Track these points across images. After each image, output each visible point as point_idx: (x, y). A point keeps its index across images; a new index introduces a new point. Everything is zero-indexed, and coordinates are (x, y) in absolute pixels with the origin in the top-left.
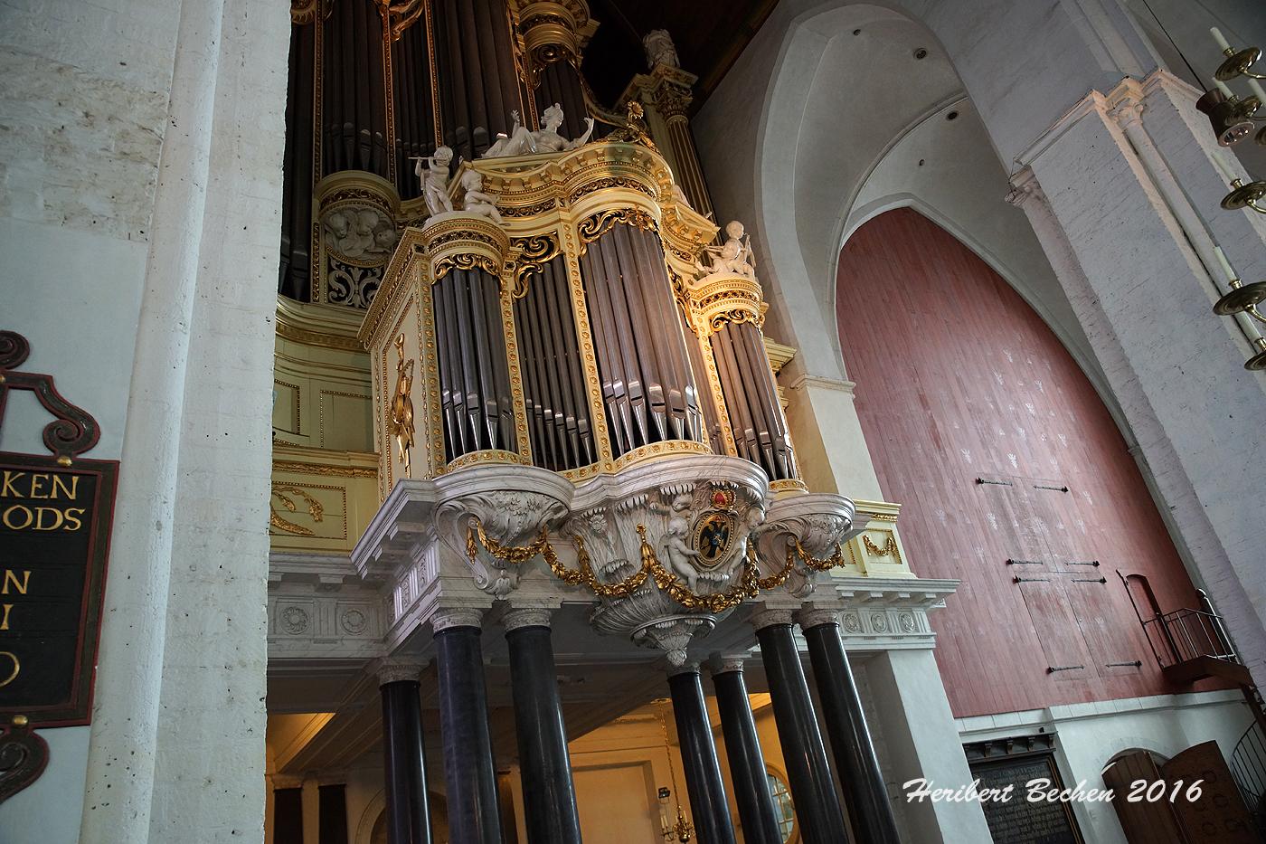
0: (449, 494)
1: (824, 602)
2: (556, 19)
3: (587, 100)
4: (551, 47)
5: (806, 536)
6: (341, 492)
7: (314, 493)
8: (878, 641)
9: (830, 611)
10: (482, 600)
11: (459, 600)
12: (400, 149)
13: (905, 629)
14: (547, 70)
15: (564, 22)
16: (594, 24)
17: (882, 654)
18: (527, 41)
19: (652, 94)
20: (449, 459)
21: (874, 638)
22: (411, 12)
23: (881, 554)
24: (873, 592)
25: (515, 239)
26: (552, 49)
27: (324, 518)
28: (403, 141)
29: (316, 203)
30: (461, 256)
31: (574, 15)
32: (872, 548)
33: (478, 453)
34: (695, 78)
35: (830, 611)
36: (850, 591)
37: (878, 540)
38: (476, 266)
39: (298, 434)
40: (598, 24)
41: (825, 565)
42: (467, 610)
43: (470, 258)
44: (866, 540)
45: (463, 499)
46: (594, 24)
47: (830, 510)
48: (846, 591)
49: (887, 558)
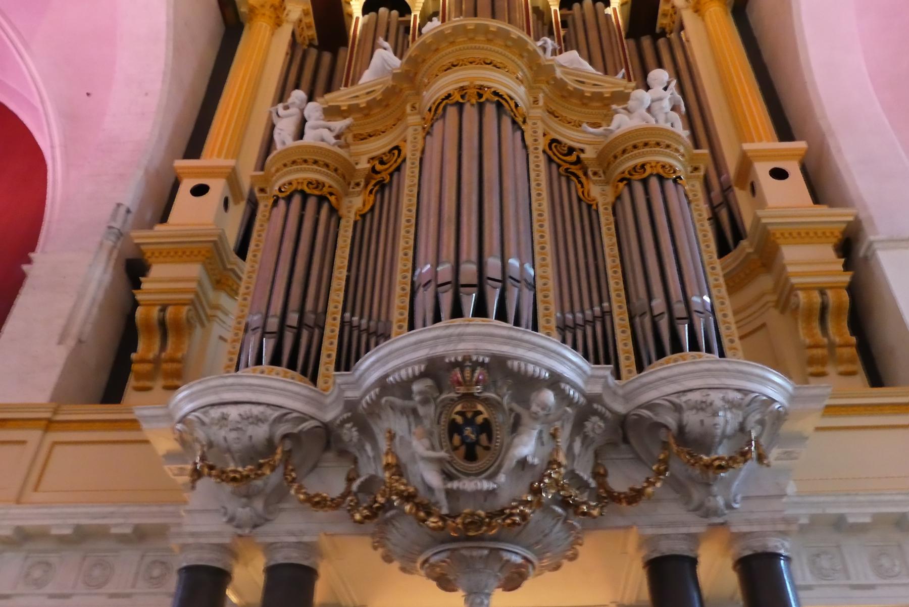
5: (681, 428)
35: (763, 534)
42: (201, 547)
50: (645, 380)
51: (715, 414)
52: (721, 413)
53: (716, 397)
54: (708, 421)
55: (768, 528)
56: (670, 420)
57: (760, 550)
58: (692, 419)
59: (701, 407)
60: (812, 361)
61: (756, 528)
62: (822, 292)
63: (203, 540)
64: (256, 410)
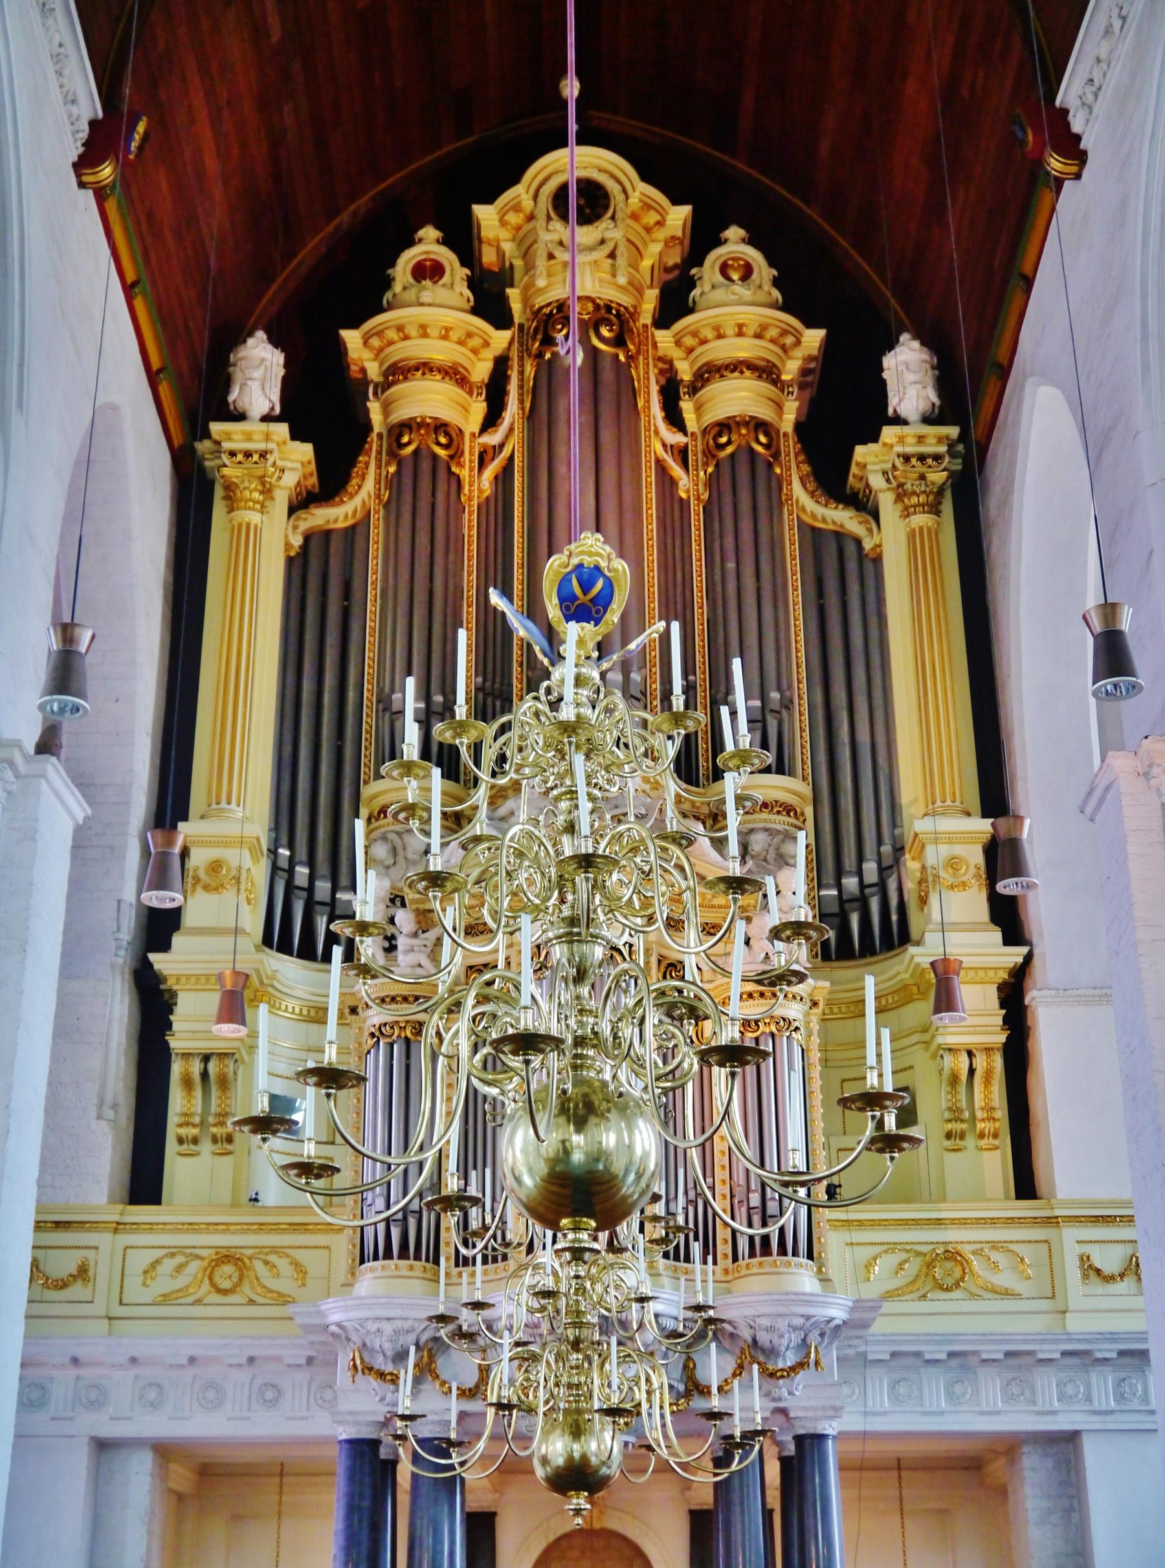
0: (335, 1318)
1: (805, 1408)
2: (736, 366)
3: (798, 491)
4: (724, 426)
5: (755, 1341)
6: (326, 1251)
7: (300, 1256)
8: (1060, 1418)
9: (816, 1419)
10: (375, 1413)
11: (351, 1413)
12: (481, 696)
13: (1120, 1397)
14: (717, 466)
15: (748, 368)
16: (814, 338)
17: (1072, 1438)
18: (698, 409)
19: (885, 473)
20: (362, 1262)
21: (1054, 1413)
22: (502, 446)
23: (1112, 1278)
24: (1042, 1351)
25: (471, 967)
26: (726, 431)
27: (308, 1281)
28: (485, 680)
29: (364, 812)
30: (385, 1025)
31: (772, 341)
32: (1090, 1271)
33: (381, 1262)
34: (953, 431)
35: (816, 1419)
36: (998, 1351)
37: (1109, 1259)
38: (399, 1036)
39: (333, 1143)
40: (820, 333)
41: (779, 1374)
42: (359, 1424)
43: (392, 1028)
44: (1084, 1259)
45: (339, 1325)
46: (814, 338)
47: (781, 1310)
48: (989, 1352)
49: (1121, 1287)
50: (729, 1301)
51: (781, 1336)
52: (786, 1336)
53: (782, 1324)
54: (776, 1340)
55: (820, 1414)
56: (746, 1334)
57: (811, 1431)
58: (764, 1338)
59: (770, 1329)
60: (949, 1136)
61: (810, 1414)
62: (970, 1054)
63: (360, 1418)
64: (407, 1325)
